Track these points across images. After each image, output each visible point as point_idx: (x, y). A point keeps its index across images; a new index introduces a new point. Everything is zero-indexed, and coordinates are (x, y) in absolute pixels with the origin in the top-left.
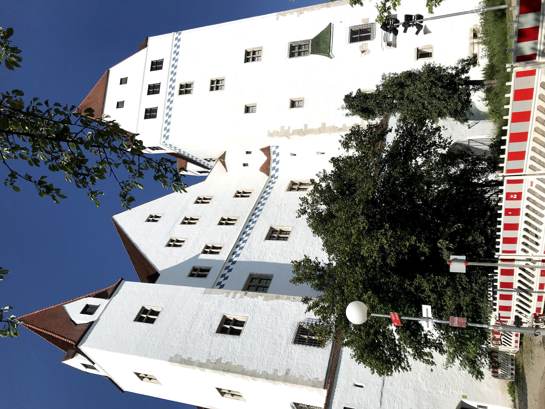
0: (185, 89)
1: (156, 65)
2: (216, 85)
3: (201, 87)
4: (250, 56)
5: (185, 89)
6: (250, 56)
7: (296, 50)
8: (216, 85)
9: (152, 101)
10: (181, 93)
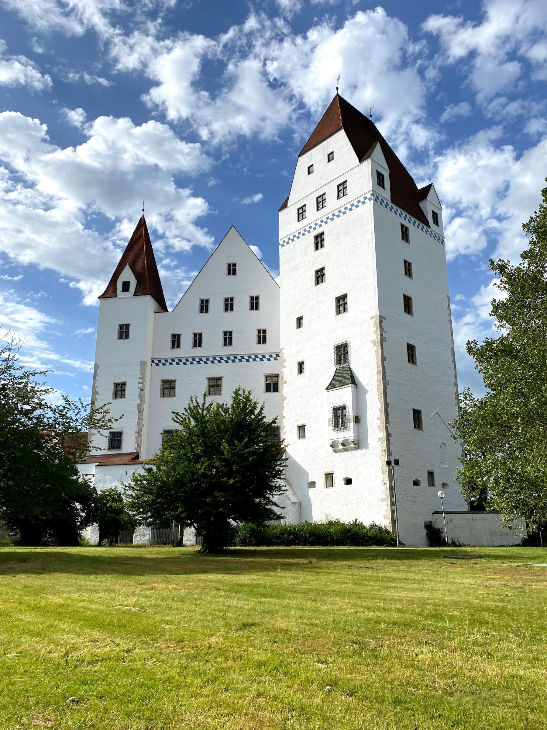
0: (319, 241)
1: (342, 189)
2: (320, 276)
3: (320, 259)
4: (341, 303)
5: (319, 241)
6: (341, 303)
7: (342, 352)
8: (320, 276)
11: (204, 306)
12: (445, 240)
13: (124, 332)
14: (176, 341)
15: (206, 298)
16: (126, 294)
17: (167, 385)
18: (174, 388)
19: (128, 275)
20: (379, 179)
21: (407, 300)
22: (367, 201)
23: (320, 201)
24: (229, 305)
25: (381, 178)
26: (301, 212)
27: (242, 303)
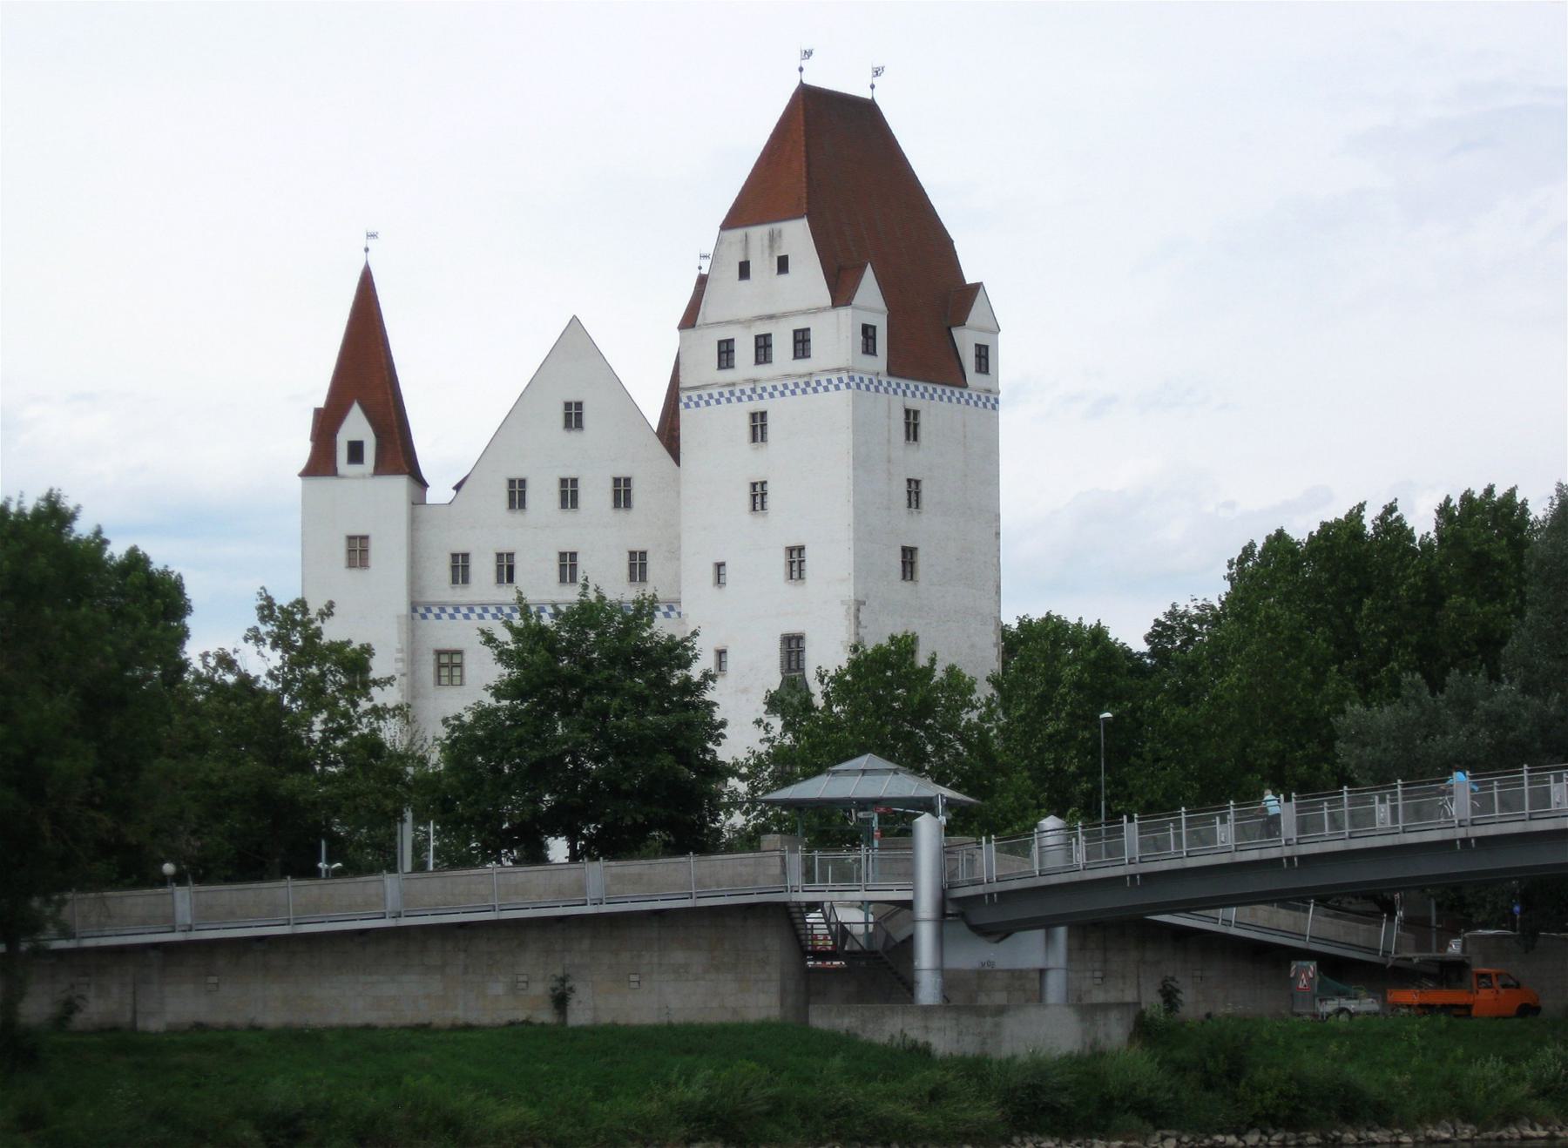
0: (758, 426)
1: (802, 343)
2: (758, 495)
4: (796, 558)
5: (758, 426)
6: (796, 558)
8: (758, 495)
9: (745, 351)
10: (753, 416)
11: (517, 494)
12: (1001, 397)
13: (358, 551)
14: (460, 567)
15: (522, 476)
16: (356, 469)
17: (444, 659)
18: (460, 665)
19: (356, 426)
20: (868, 332)
21: (909, 556)
22: (842, 386)
23: (763, 347)
24: (569, 494)
25: (870, 333)
26: (726, 353)
27: (595, 495)
